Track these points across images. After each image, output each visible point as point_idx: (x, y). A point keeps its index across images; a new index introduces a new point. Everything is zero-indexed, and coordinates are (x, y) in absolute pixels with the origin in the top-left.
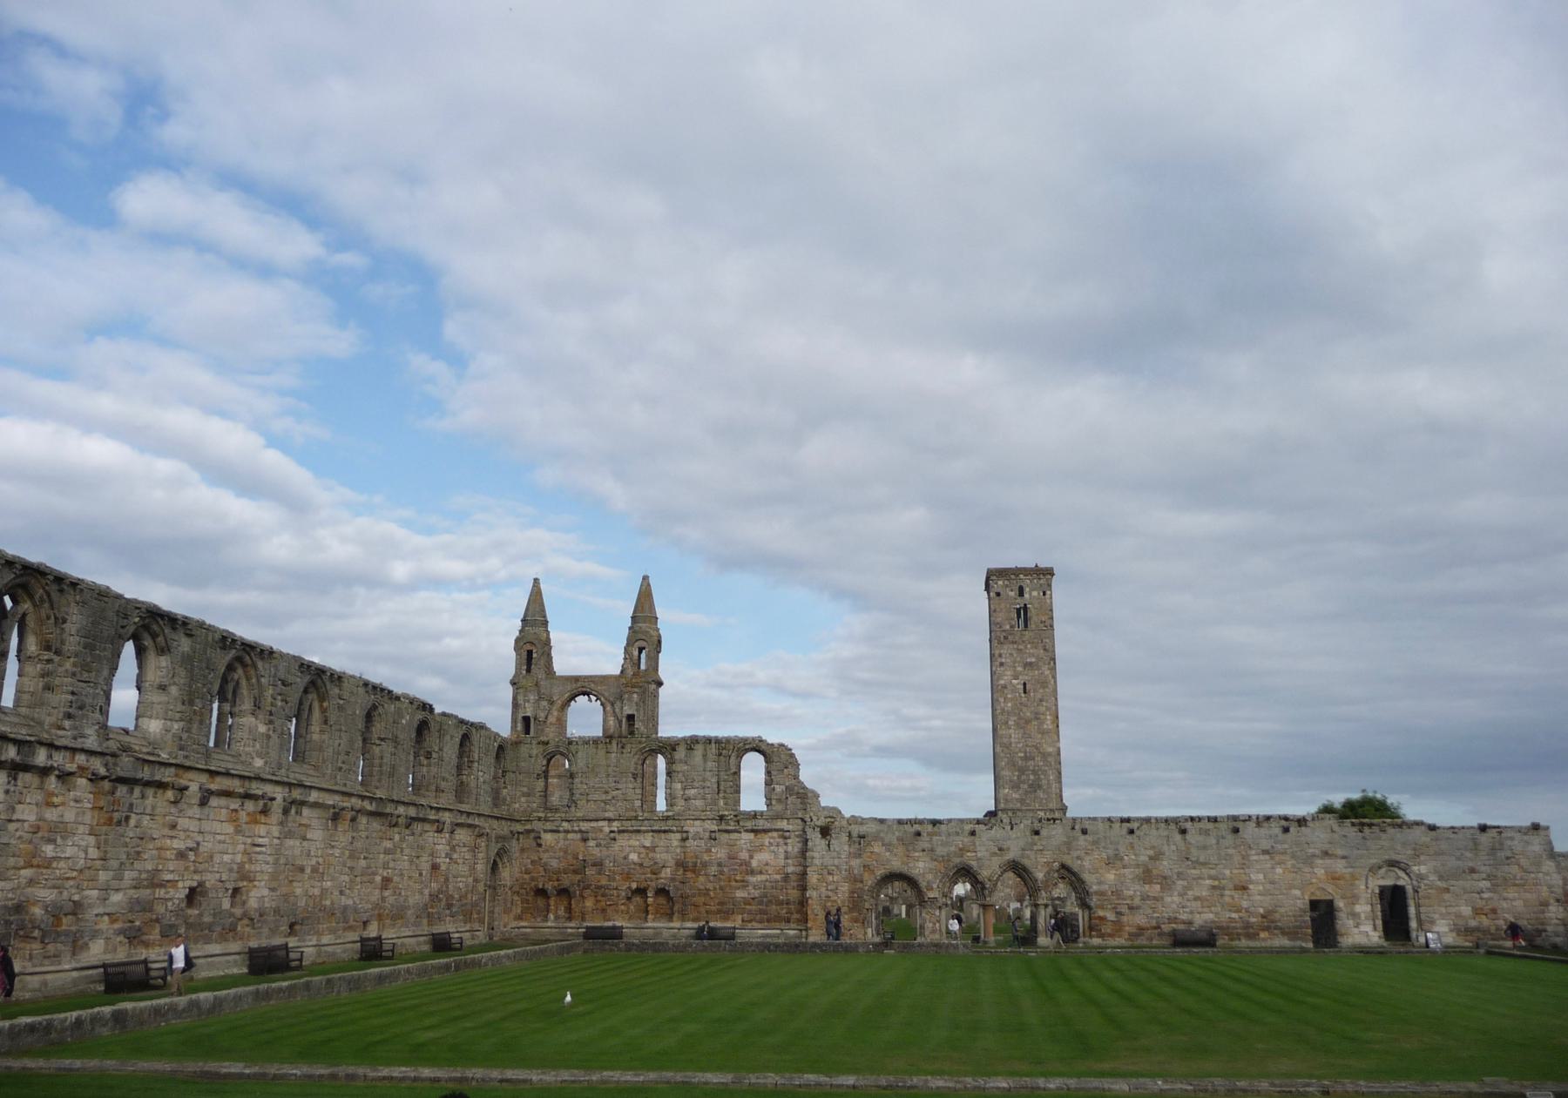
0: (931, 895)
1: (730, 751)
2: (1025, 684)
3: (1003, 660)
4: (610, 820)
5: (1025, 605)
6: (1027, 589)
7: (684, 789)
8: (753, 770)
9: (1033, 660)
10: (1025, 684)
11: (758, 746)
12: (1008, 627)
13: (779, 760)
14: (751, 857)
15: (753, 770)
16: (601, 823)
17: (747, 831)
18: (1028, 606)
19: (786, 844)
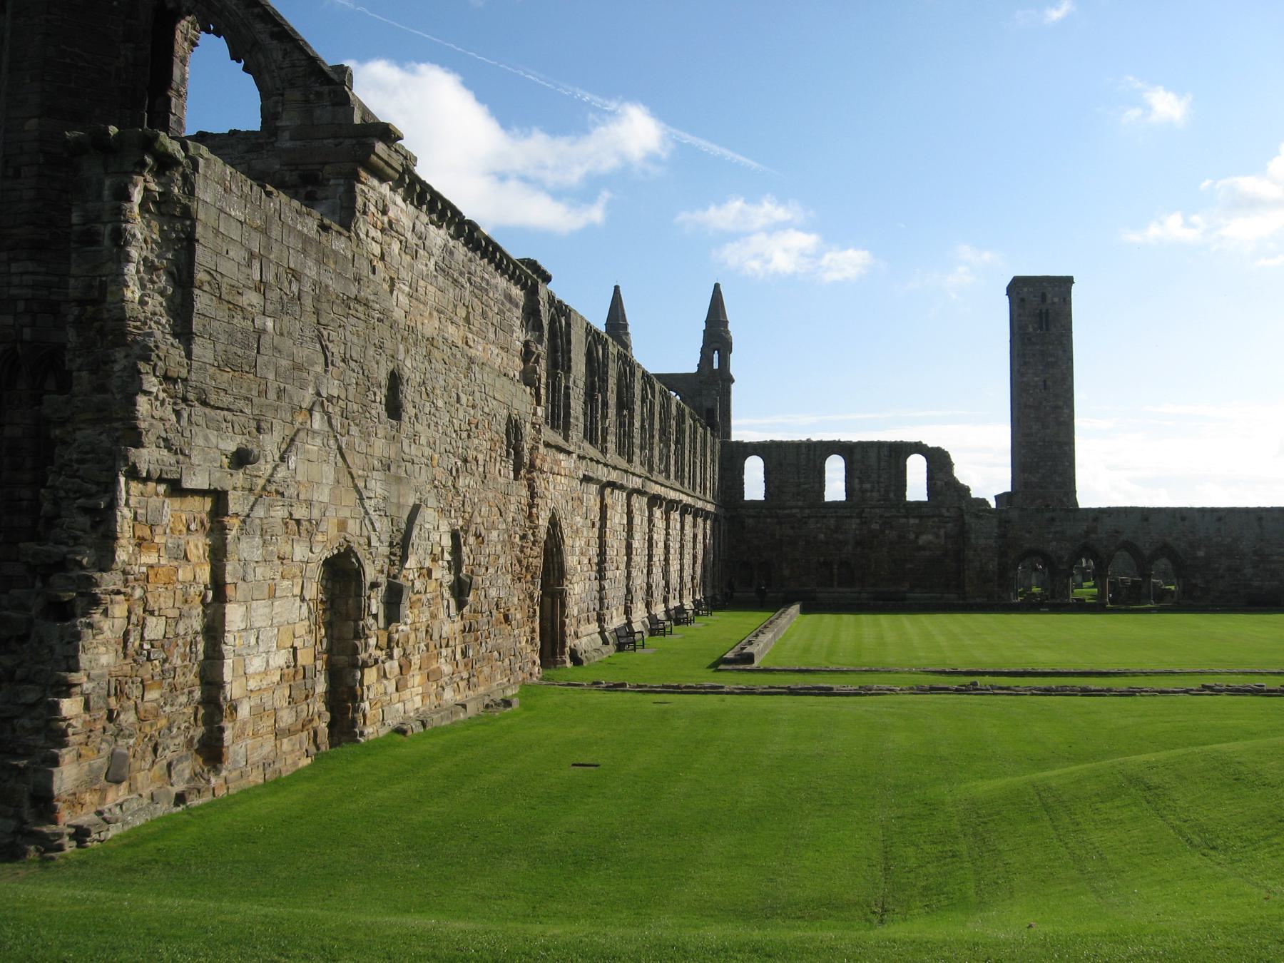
0: (1061, 567)
1: (899, 452)
2: (1045, 381)
3: (1027, 360)
4: (802, 508)
5: (1047, 310)
6: (1050, 296)
7: (861, 482)
8: (916, 468)
9: (1053, 360)
10: (1045, 381)
11: (918, 448)
12: (1031, 330)
13: (939, 461)
14: (917, 537)
15: (916, 468)
16: (794, 511)
17: (913, 517)
18: (1050, 311)
19: (945, 527)
